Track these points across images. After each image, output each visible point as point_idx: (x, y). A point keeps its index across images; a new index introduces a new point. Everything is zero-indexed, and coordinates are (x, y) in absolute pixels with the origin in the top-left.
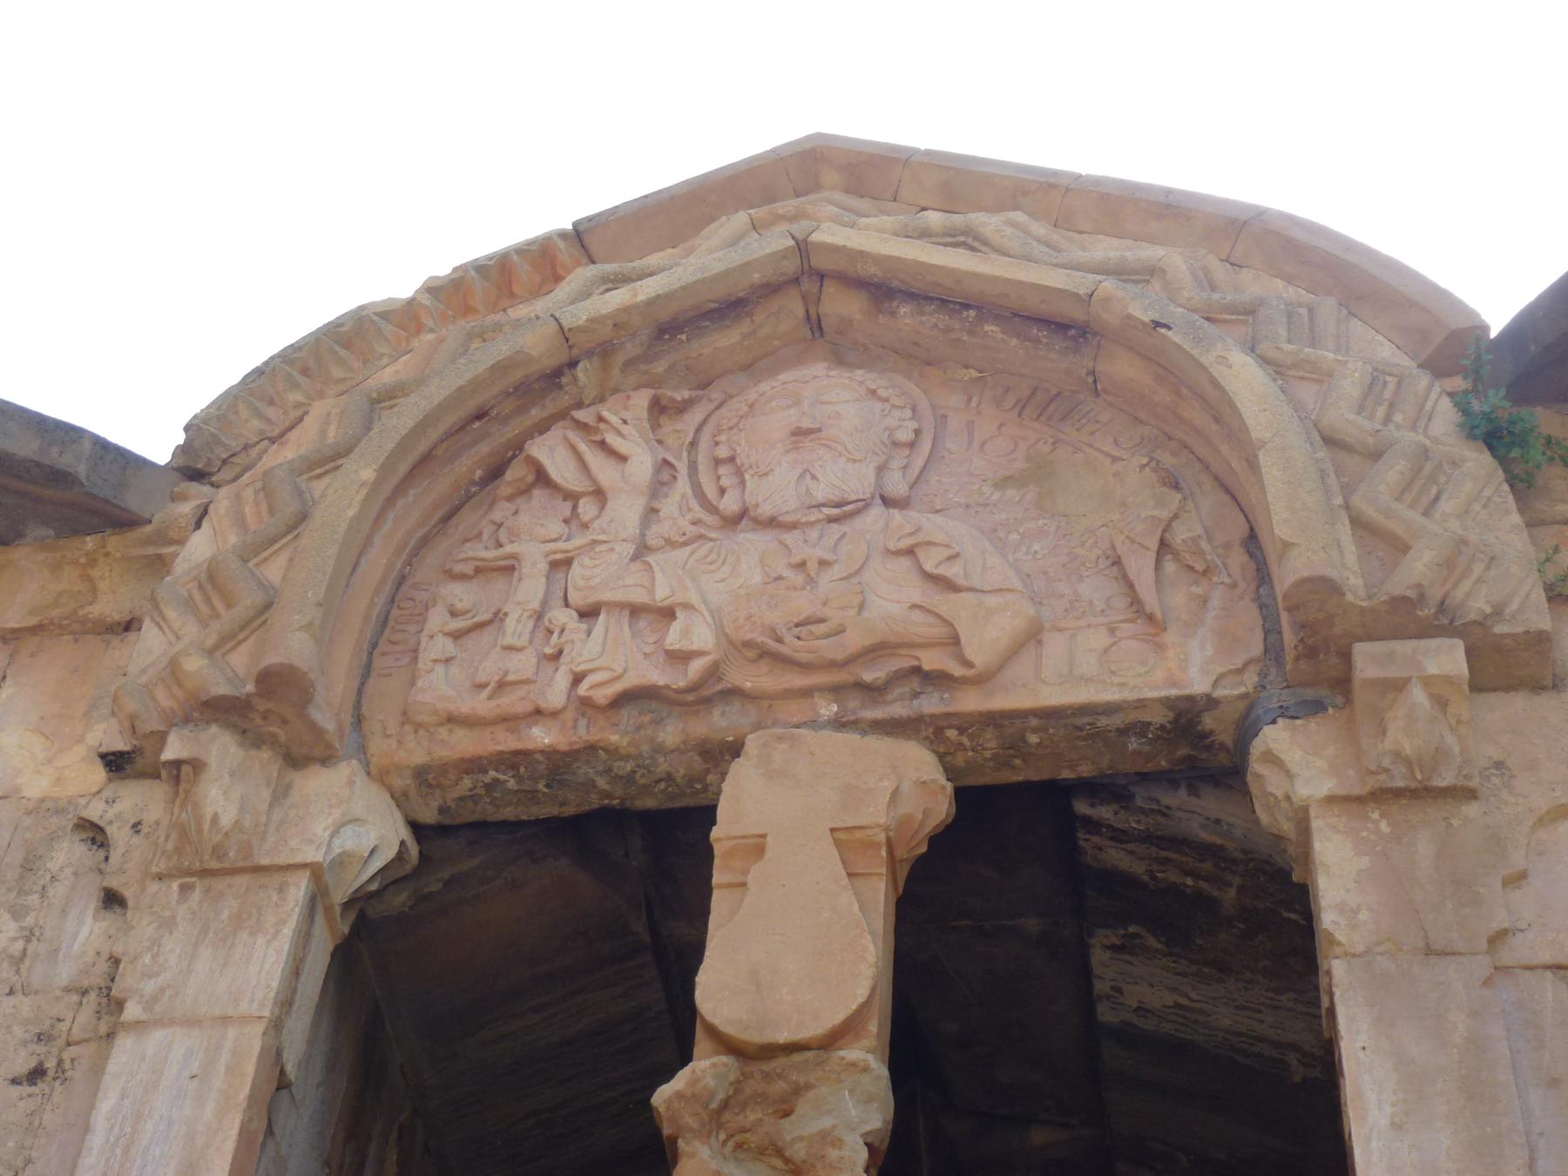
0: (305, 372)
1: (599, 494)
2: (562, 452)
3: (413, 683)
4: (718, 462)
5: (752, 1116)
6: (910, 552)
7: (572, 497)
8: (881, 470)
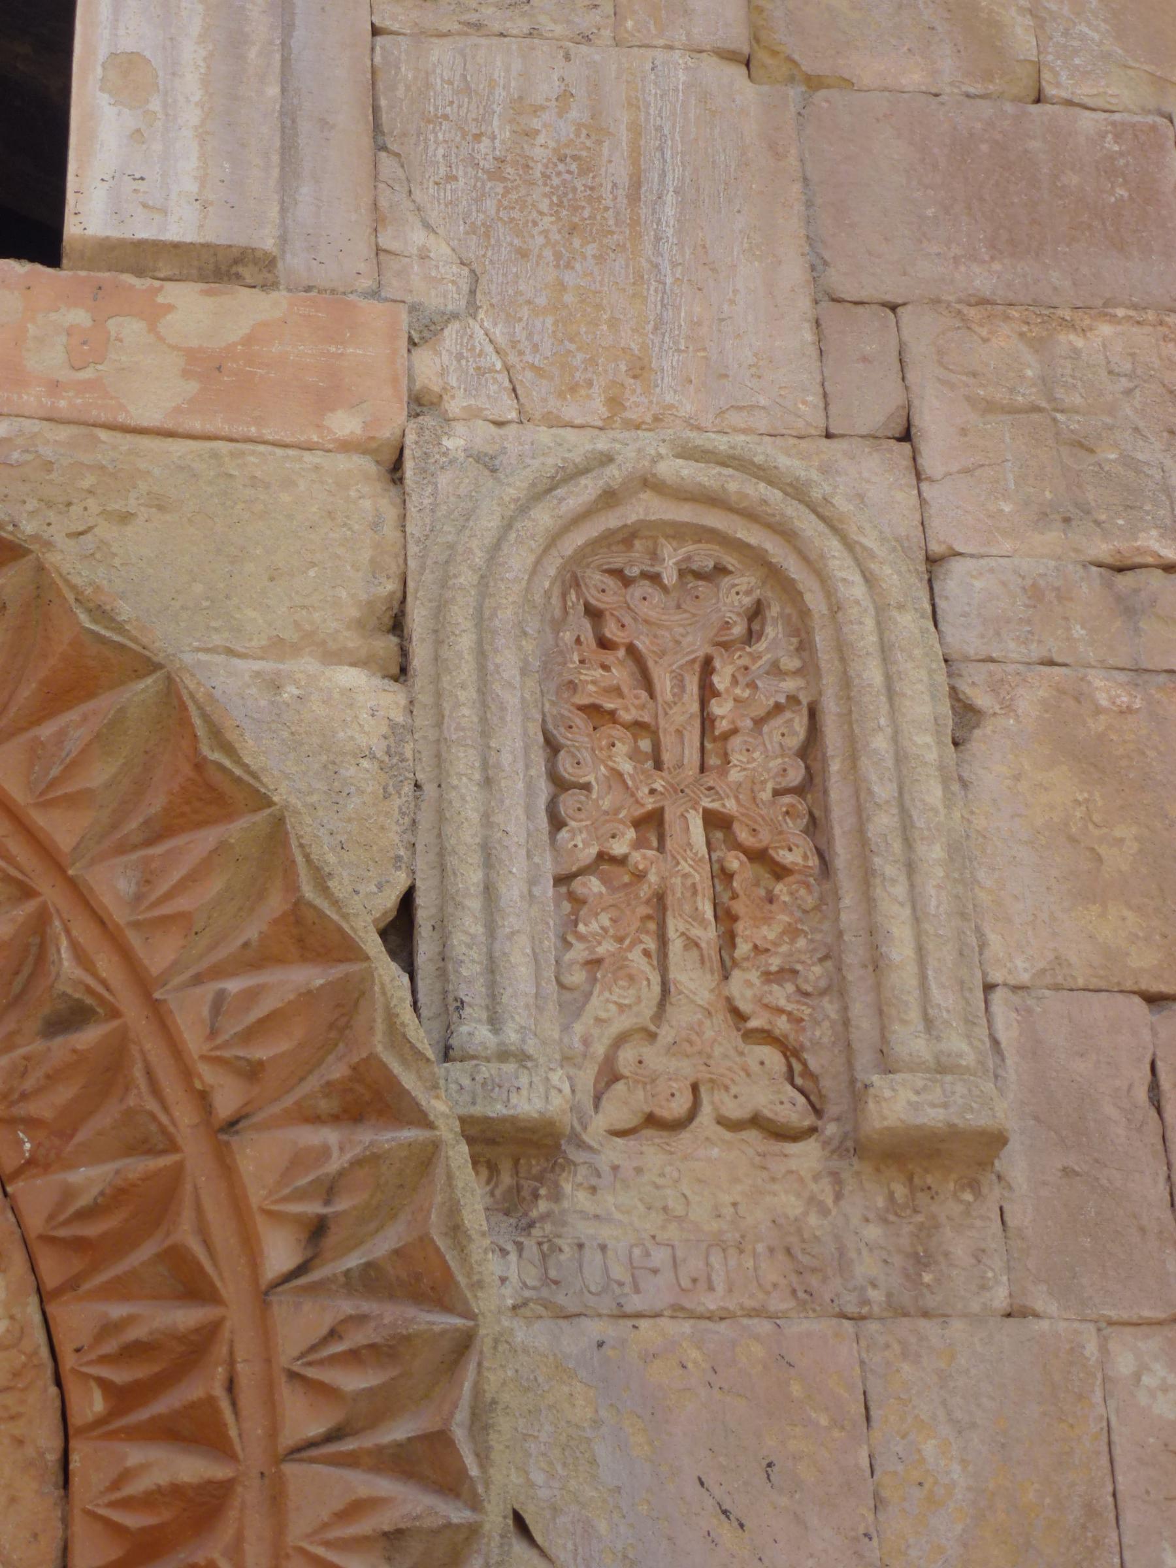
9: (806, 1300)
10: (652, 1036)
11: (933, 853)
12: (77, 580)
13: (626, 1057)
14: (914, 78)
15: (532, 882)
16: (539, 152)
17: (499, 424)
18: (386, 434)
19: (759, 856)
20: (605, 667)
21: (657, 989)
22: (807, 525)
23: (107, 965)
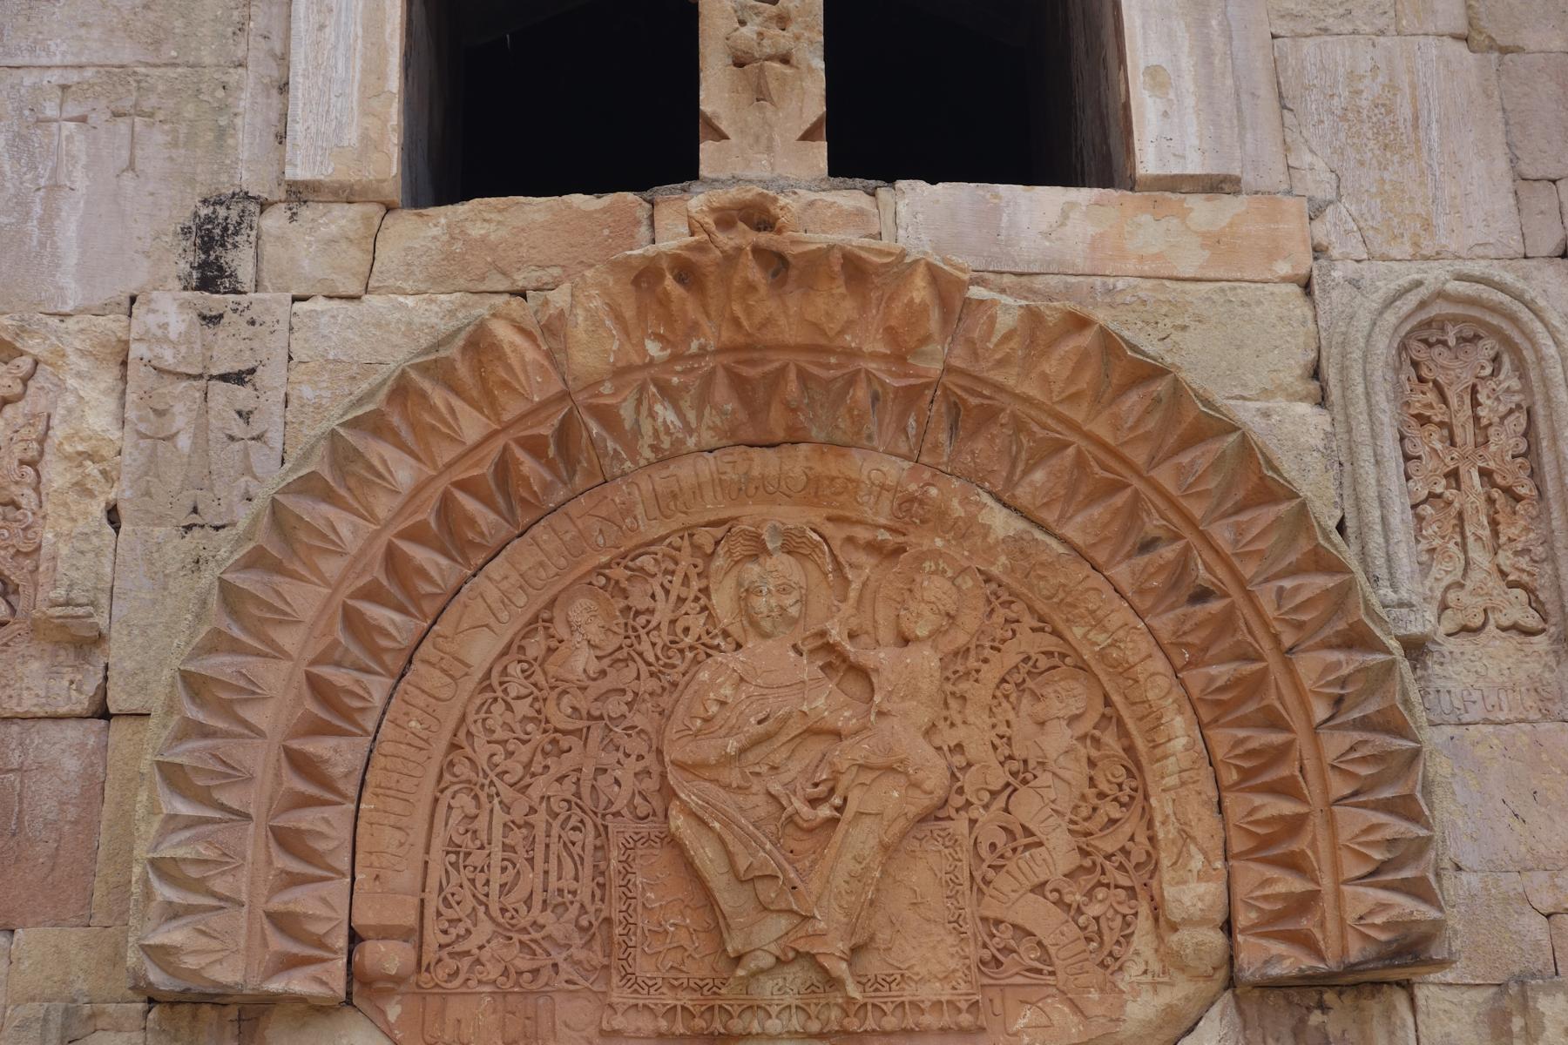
9: (1546, 715)
10: (1462, 586)
12: (1194, 386)
13: (1452, 596)
15: (1403, 512)
17: (1358, 261)
18: (1303, 271)
19: (1507, 491)
20: (1424, 393)
21: (1463, 562)
22: (1525, 315)
23: (1221, 571)
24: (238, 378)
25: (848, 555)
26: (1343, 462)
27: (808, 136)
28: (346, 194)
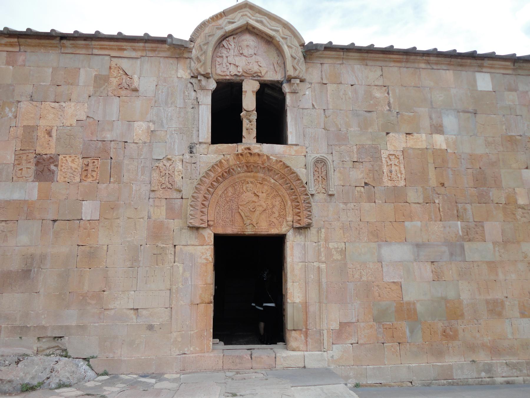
0: (200, 28)
1: (229, 49)
2: (226, 44)
3: (216, 70)
4: (239, 46)
5: (248, 116)
6: (257, 62)
7: (227, 49)
8: (254, 50)
9: (326, 202)
11: (332, 179)
14: (333, 130)
16: (313, 136)
18: (305, 155)
22: (327, 160)
24: (194, 163)
25: (257, 184)
26: (307, 175)
27: (254, 138)
28: (205, 143)
